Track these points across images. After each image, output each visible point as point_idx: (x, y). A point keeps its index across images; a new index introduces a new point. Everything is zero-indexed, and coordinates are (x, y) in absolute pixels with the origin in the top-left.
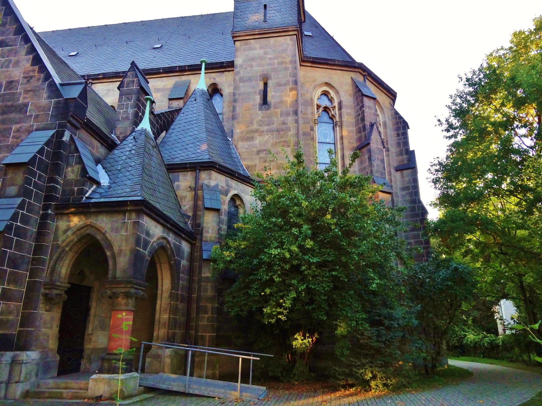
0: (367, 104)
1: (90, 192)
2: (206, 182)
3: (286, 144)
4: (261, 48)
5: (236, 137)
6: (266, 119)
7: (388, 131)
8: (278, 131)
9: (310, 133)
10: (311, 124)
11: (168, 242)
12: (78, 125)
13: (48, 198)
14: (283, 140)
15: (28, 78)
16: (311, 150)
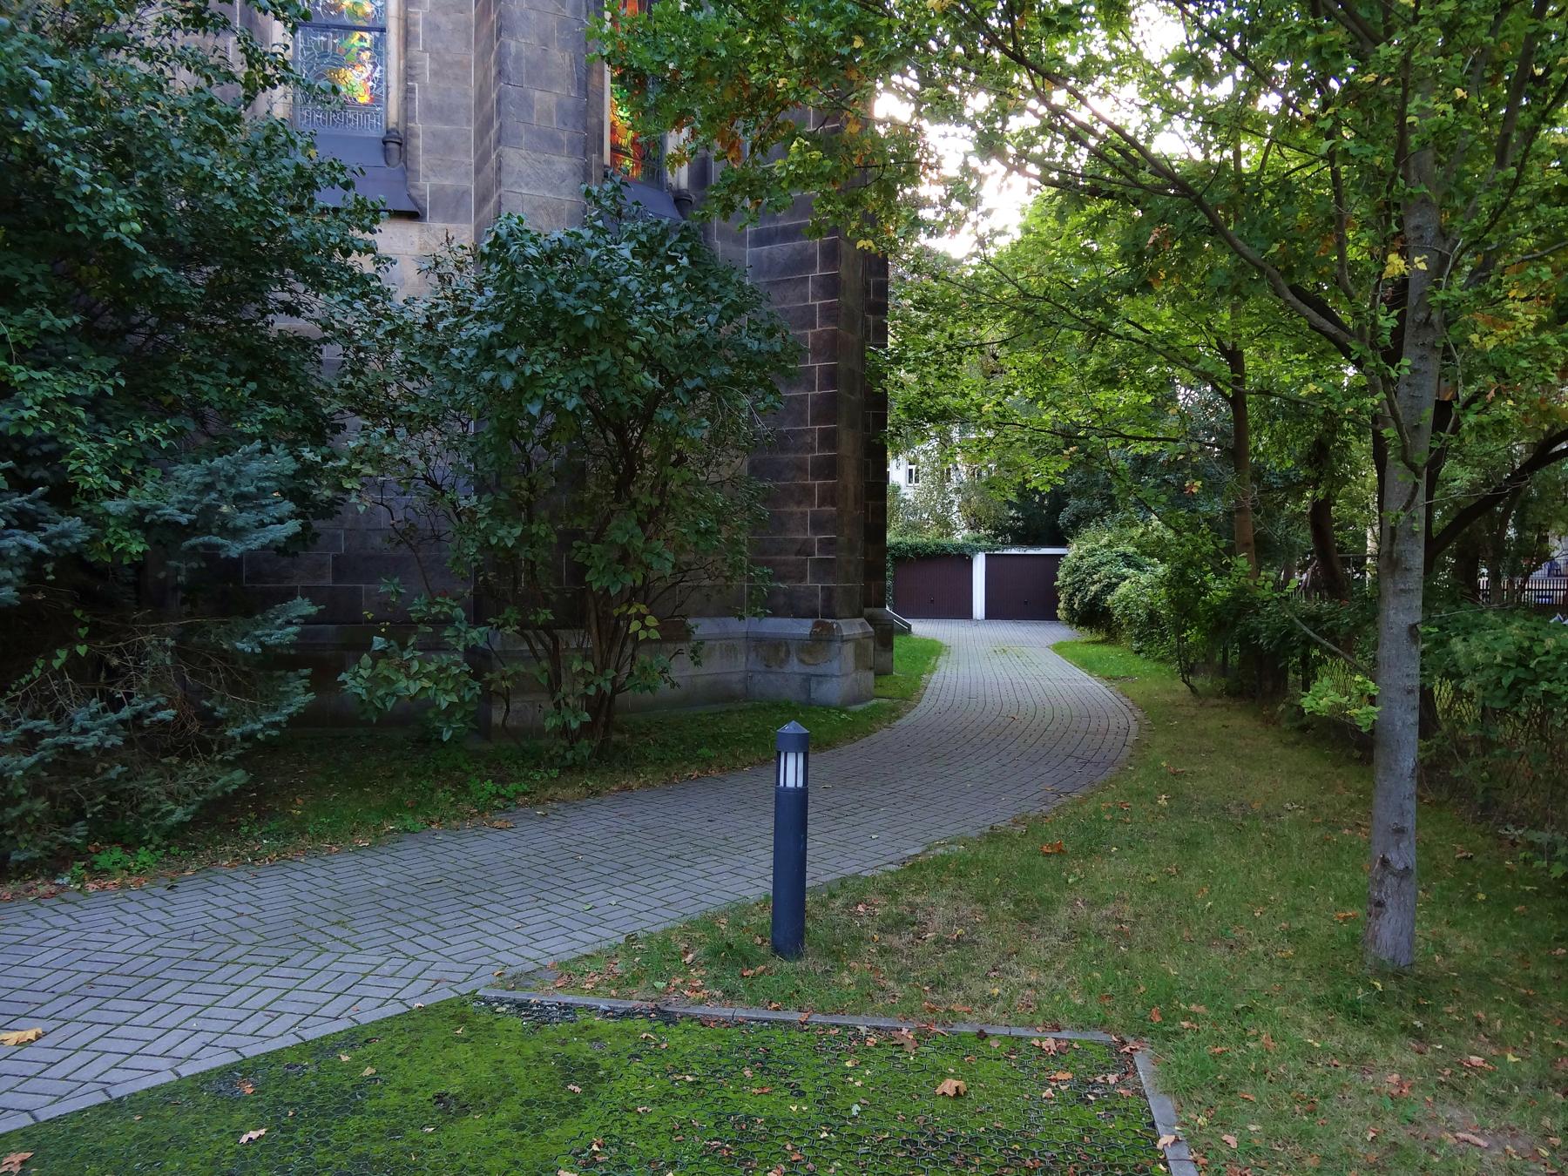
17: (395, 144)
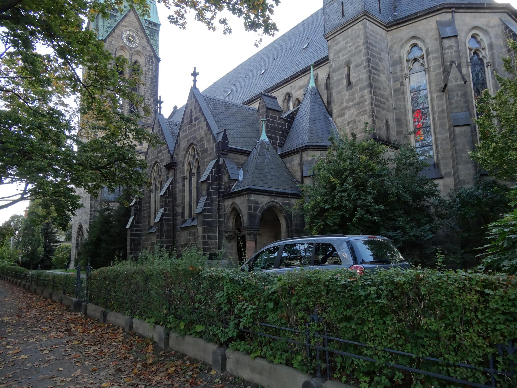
0: (448, 45)
2: (306, 159)
3: (364, 112)
4: (343, 40)
5: (334, 116)
6: (351, 97)
7: (495, 51)
8: (358, 104)
10: (400, 80)
11: (277, 203)
12: (226, 153)
13: (219, 193)
14: (362, 110)
15: (206, 134)
16: (402, 103)
17: (436, 166)
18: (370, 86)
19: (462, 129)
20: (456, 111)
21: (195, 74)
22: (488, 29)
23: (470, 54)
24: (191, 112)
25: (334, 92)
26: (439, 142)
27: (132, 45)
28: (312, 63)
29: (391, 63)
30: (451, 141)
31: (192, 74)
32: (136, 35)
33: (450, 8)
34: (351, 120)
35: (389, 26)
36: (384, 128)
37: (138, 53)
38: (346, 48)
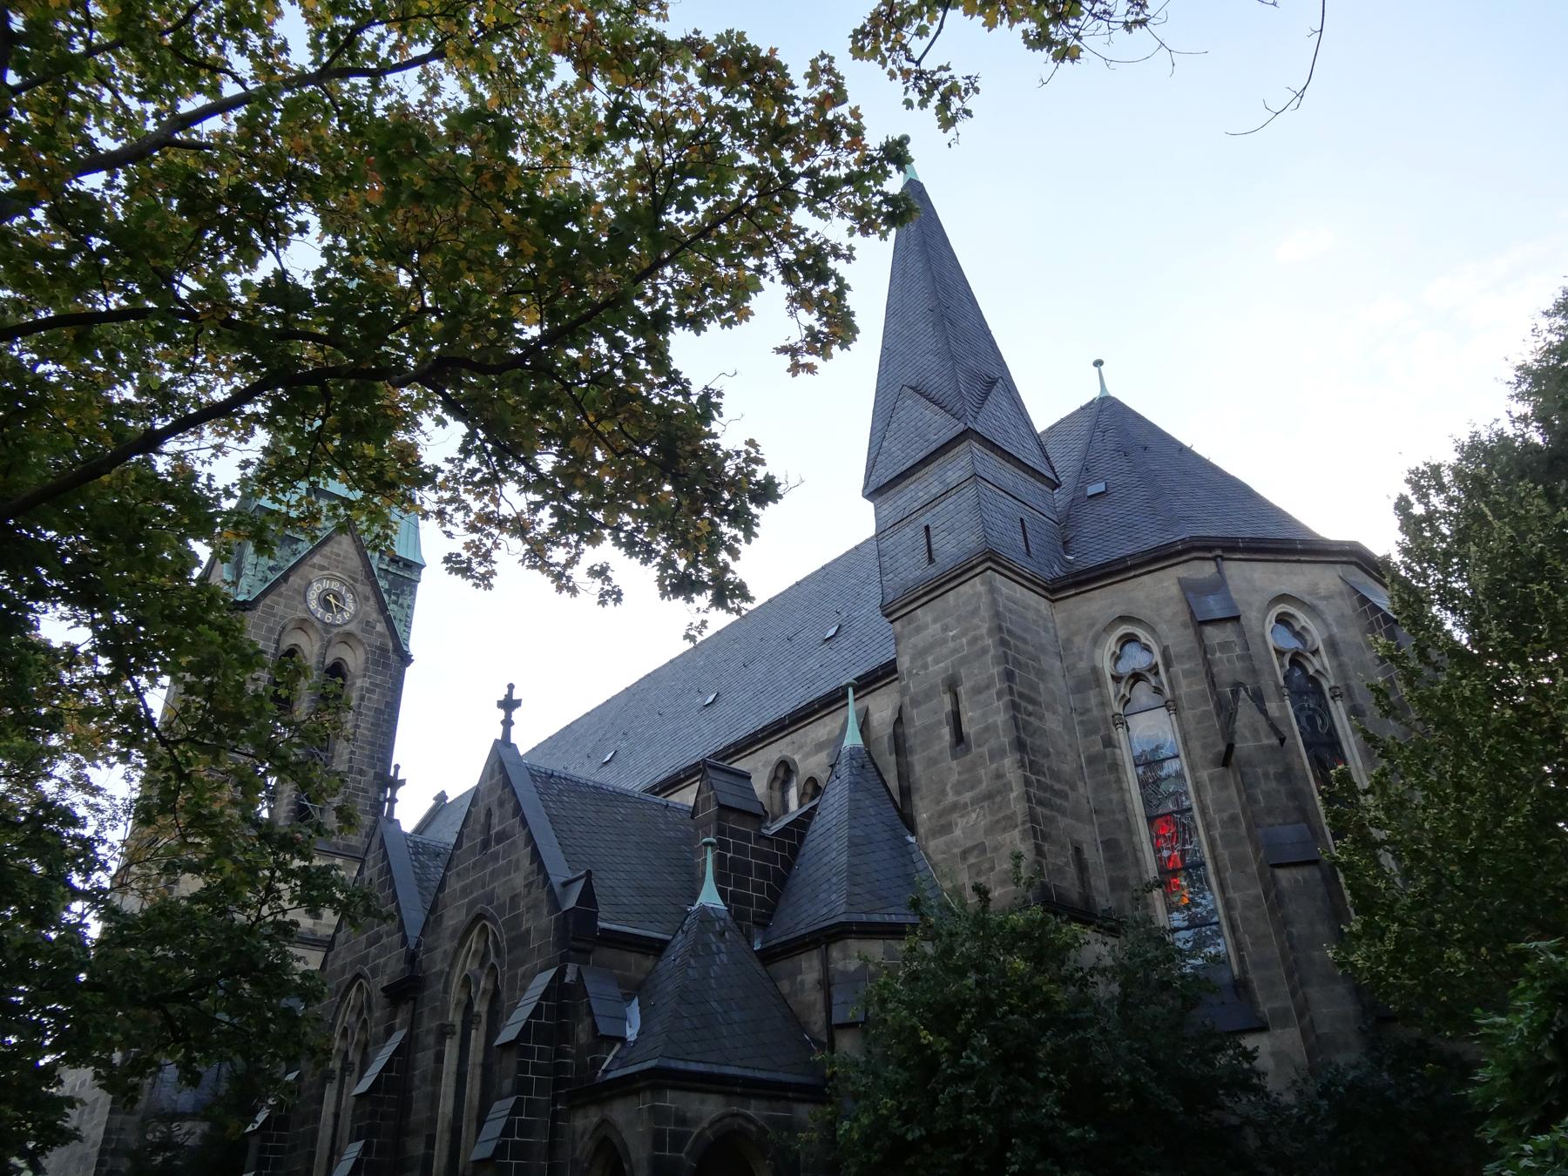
1: (610, 1058)
2: (840, 966)
3: (1008, 823)
4: (935, 621)
5: (921, 831)
6: (965, 776)
7: (1345, 659)
8: (989, 796)
9: (1104, 756)
11: (749, 1119)
13: (558, 1084)
14: (1001, 815)
15: (529, 886)
16: (1115, 797)
17: (1241, 987)
18: (1020, 745)
19: (1300, 874)
20: (1269, 820)
21: (509, 704)
22: (1316, 602)
23: (1282, 666)
24: (489, 814)
25: (918, 761)
26: (1236, 914)
27: (334, 618)
28: (849, 679)
29: (1071, 683)
30: (1272, 910)
31: (501, 704)
32: (349, 590)
33: (1210, 549)
34: (972, 844)
35: (1055, 590)
36: (1072, 870)
37: (347, 638)
38: (945, 641)
